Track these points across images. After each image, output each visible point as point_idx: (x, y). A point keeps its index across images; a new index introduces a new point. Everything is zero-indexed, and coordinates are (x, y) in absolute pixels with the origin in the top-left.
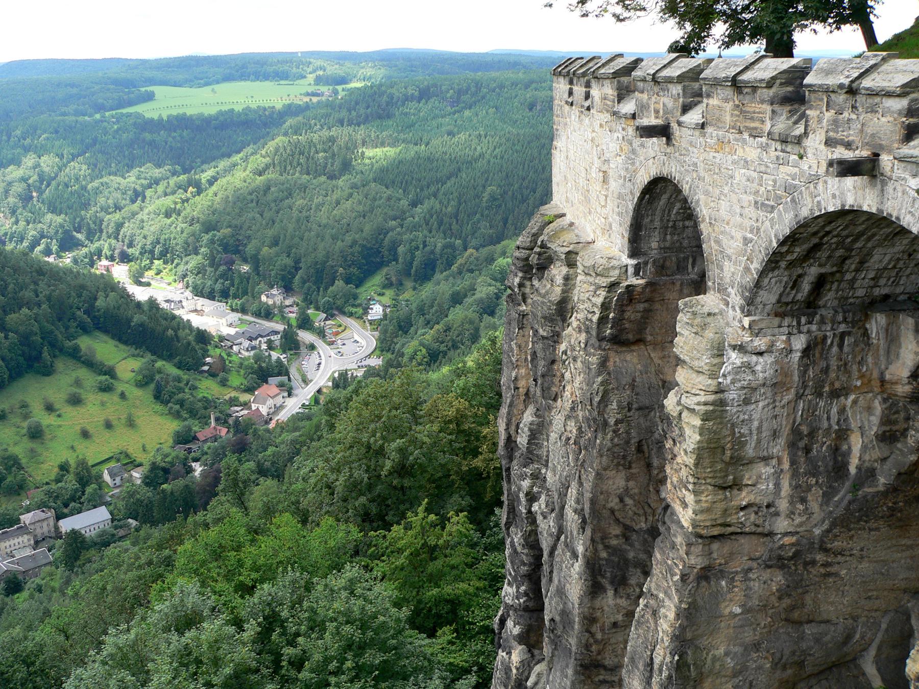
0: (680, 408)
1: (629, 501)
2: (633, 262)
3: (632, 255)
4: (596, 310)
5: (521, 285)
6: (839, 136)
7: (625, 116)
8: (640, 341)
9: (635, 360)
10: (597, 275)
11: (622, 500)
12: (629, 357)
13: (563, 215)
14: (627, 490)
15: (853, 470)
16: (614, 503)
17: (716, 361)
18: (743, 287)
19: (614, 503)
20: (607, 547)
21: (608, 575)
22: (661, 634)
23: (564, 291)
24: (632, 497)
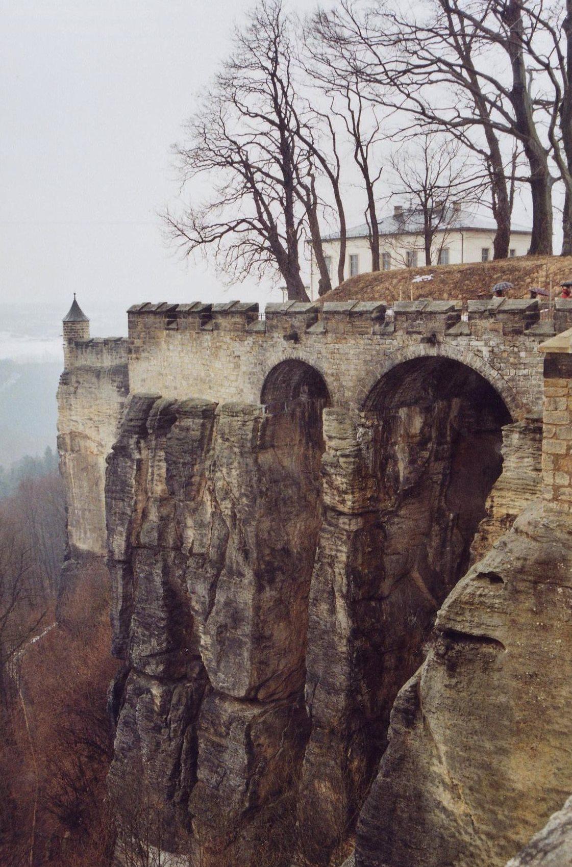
0: (336, 458)
1: (273, 534)
2: (264, 406)
3: (262, 402)
4: (248, 433)
5: (138, 443)
6: (415, 330)
7: (257, 332)
8: (273, 446)
9: (270, 457)
10: (245, 414)
11: (269, 533)
12: (266, 455)
13: (160, 397)
14: (271, 527)
15: (401, 479)
16: (266, 536)
17: (354, 432)
18: (358, 401)
19: (266, 536)
20: (264, 561)
21: (266, 578)
22: (337, 570)
23: (202, 433)
24: (274, 531)
